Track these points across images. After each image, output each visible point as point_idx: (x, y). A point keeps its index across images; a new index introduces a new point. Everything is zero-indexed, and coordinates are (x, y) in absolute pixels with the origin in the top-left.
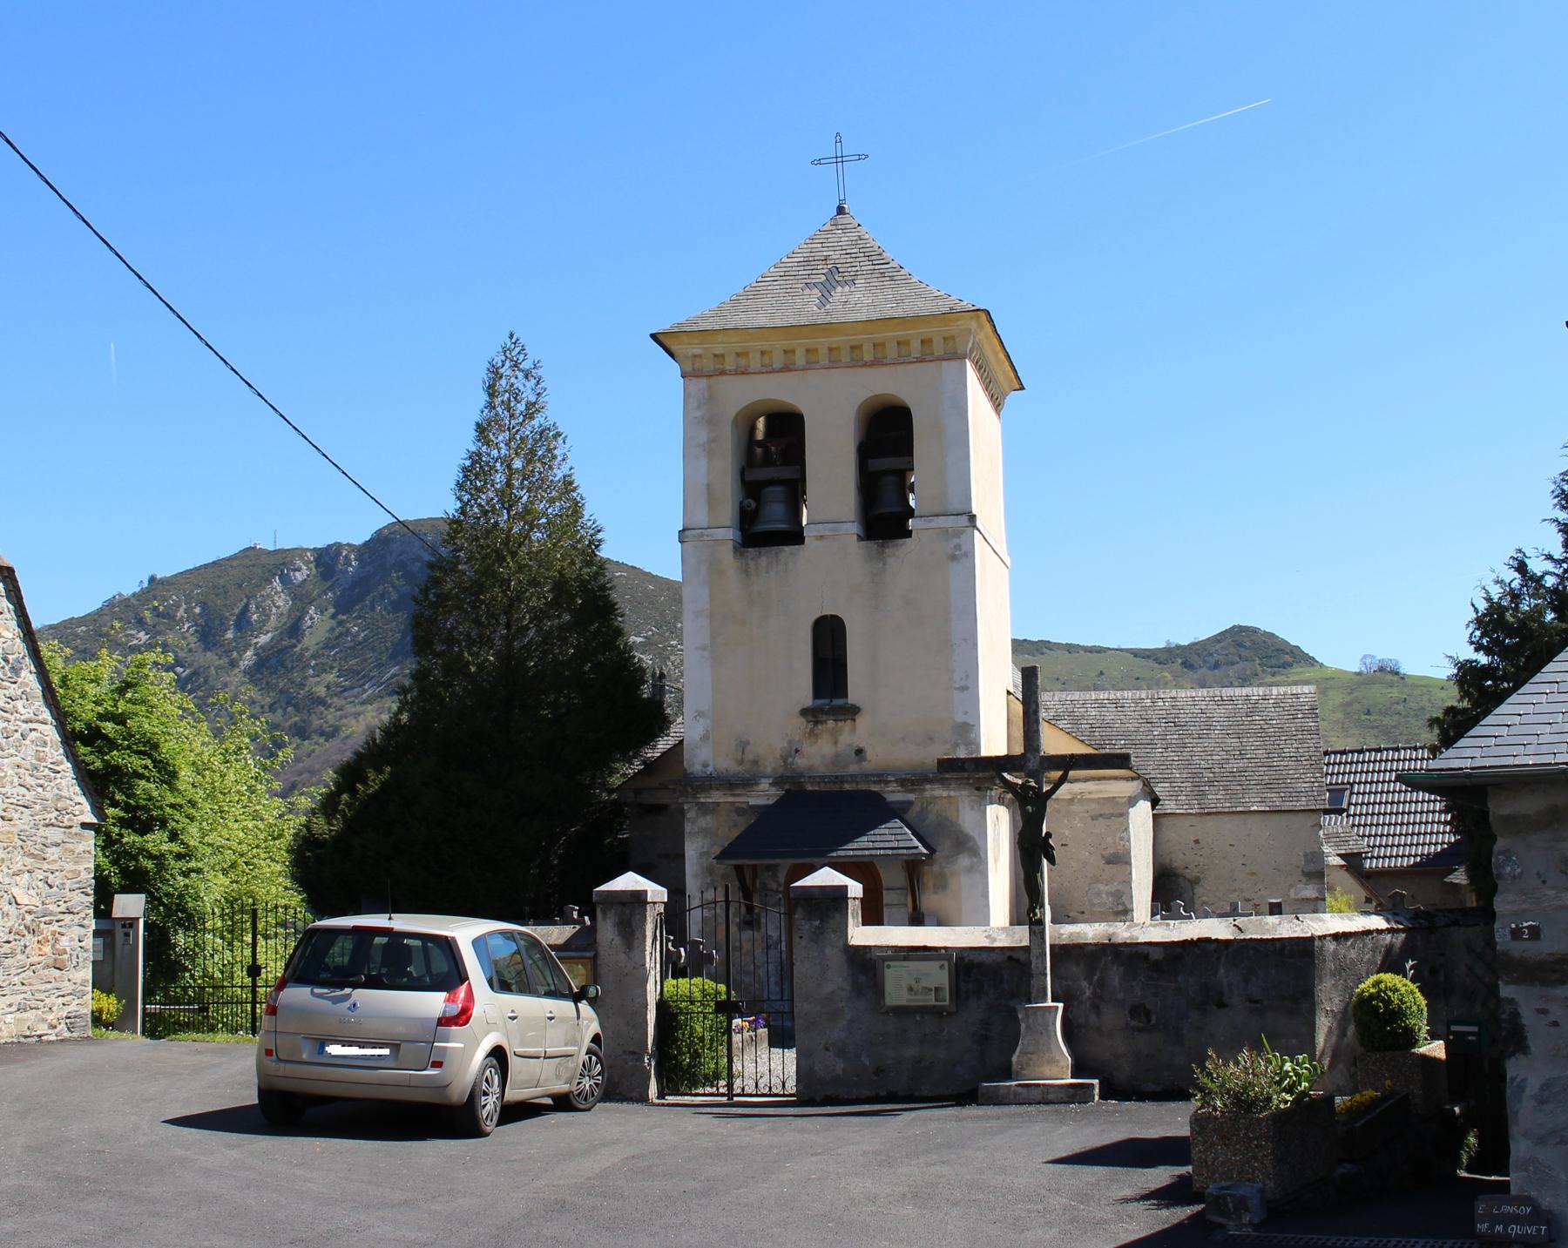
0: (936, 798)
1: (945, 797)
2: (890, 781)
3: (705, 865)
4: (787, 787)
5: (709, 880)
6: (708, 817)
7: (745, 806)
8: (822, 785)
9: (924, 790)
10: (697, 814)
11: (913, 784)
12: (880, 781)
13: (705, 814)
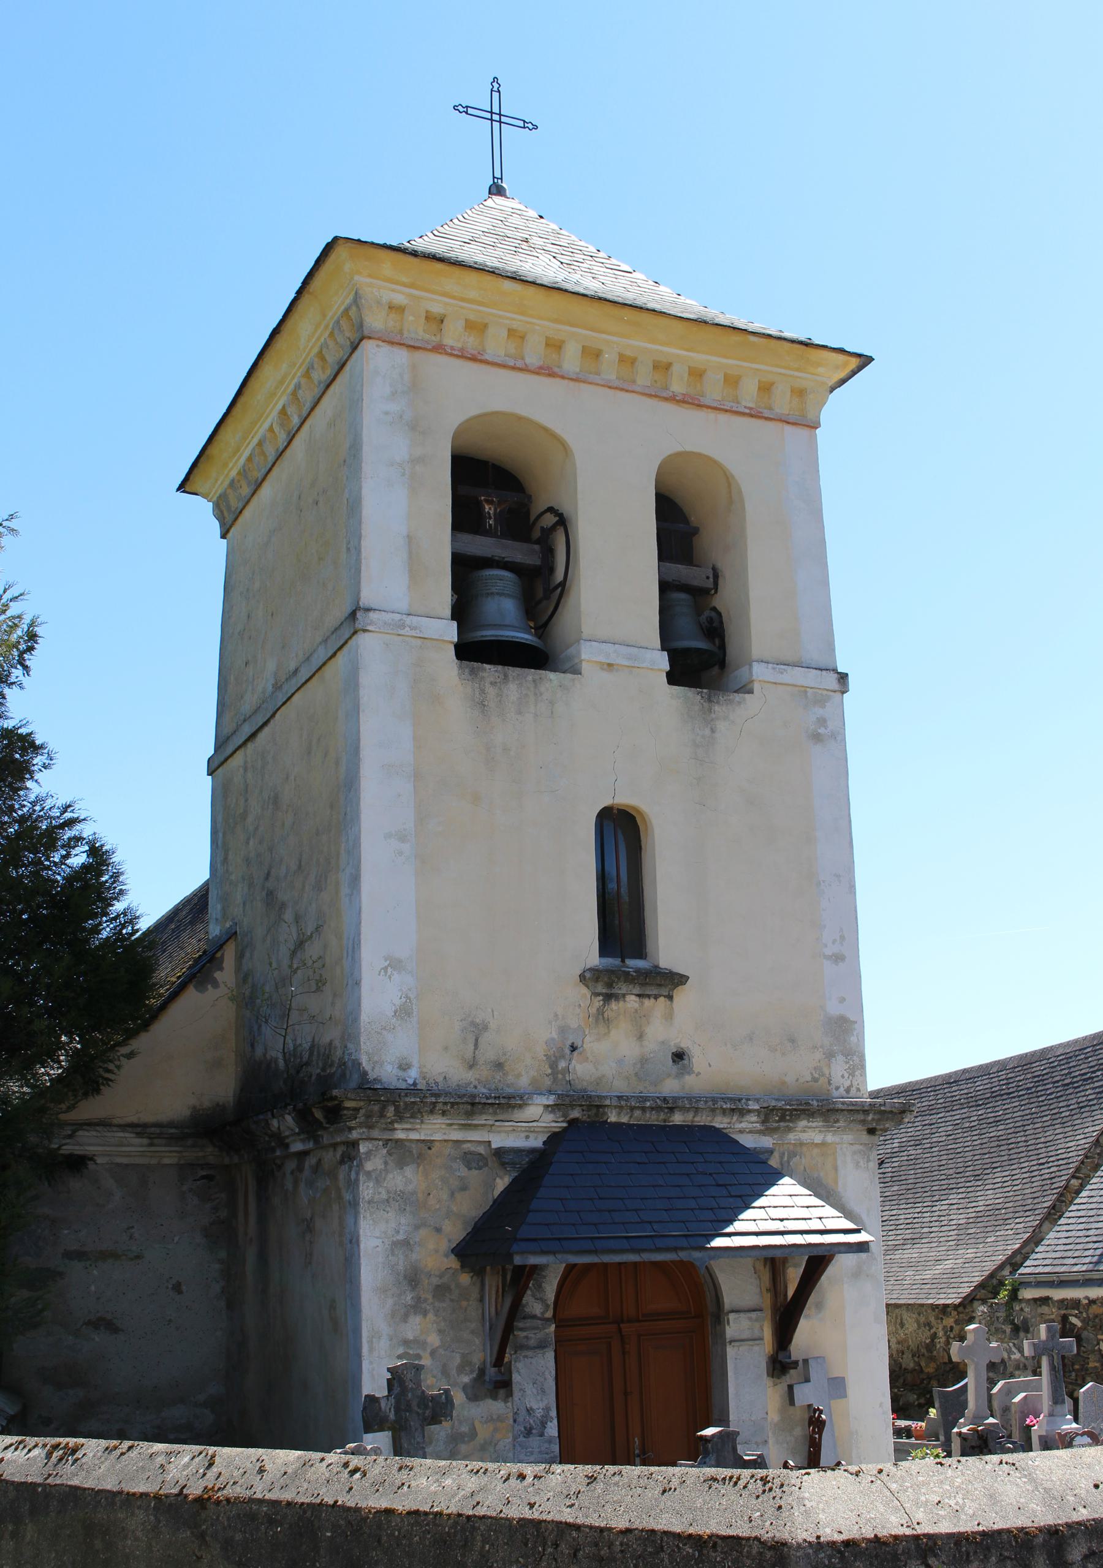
0: (802, 1144)
1: (817, 1145)
2: (749, 1111)
3: (401, 1268)
4: (575, 1114)
5: (409, 1298)
6: (409, 1171)
7: (481, 1149)
8: (637, 1113)
9: (789, 1130)
10: (386, 1163)
11: (782, 1119)
12: (733, 1110)
13: (401, 1164)
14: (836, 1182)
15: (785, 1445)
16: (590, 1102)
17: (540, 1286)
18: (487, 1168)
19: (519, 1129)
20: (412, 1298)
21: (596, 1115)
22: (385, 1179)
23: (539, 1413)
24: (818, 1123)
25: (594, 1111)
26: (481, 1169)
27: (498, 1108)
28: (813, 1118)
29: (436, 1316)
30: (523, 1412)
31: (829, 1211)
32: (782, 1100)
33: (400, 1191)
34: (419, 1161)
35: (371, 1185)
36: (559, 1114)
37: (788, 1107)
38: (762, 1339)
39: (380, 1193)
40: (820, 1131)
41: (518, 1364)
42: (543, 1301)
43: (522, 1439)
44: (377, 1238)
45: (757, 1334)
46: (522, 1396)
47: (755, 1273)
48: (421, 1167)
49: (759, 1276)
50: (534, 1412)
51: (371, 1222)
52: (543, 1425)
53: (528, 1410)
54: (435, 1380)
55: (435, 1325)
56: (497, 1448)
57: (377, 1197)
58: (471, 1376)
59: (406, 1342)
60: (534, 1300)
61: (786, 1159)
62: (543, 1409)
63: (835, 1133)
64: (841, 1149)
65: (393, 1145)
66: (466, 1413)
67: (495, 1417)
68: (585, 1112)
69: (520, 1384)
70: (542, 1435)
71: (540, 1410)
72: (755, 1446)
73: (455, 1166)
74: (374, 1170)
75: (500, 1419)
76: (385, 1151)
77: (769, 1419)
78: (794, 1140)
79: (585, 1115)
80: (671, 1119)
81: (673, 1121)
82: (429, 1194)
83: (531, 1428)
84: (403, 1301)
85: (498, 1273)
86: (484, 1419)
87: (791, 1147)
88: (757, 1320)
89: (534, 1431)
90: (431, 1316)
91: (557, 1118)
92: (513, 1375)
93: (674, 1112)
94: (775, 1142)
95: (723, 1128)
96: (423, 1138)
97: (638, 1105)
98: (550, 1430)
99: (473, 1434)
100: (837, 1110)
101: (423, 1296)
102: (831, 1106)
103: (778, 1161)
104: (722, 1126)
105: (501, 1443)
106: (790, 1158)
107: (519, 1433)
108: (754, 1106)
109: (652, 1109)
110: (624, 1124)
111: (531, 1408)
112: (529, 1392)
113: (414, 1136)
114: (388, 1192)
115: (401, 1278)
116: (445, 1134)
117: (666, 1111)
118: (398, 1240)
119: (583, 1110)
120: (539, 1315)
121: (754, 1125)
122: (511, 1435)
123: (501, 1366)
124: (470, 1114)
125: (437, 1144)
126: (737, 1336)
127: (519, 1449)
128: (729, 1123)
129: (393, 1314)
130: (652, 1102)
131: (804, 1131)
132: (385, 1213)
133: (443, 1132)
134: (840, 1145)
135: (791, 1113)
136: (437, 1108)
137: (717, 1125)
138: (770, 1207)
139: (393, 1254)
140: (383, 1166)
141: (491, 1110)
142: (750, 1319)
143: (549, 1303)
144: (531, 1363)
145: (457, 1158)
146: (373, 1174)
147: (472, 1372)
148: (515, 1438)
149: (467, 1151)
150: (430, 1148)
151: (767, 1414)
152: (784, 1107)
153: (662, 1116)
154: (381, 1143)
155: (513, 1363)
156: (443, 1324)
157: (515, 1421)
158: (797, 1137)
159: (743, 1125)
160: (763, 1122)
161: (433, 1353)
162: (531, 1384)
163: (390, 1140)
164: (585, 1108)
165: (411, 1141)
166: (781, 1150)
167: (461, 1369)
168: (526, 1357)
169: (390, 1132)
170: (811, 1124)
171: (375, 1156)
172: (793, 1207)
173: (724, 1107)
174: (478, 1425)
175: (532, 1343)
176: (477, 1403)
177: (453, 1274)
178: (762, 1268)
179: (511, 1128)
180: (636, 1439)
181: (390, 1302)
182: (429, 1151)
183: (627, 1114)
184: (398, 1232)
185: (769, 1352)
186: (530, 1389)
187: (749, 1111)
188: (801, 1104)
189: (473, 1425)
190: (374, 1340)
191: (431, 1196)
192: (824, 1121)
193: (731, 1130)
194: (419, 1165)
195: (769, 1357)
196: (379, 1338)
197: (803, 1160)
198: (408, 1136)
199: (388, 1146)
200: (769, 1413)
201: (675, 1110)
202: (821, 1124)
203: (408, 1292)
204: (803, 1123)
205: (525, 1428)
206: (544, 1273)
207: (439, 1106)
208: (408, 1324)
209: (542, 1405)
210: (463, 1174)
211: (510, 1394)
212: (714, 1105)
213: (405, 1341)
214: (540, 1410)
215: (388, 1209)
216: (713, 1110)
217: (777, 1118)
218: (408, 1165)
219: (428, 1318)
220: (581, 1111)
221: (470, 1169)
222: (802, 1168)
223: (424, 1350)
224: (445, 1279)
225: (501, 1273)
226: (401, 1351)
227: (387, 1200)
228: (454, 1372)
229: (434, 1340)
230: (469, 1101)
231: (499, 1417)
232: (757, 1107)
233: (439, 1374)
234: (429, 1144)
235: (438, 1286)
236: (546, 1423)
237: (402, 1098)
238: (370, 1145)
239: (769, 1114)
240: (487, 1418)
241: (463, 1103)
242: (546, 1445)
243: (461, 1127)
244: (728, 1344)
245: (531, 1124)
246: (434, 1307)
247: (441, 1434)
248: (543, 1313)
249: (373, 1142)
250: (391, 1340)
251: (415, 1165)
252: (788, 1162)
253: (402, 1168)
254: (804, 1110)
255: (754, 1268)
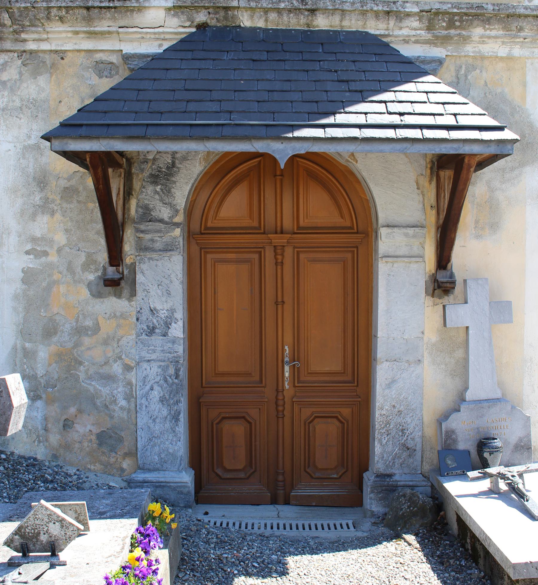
0: (483, 58)
1: (502, 58)
2: (408, 15)
3: (31, 170)
4: (201, 17)
5: (37, 198)
6: (42, 80)
7: (114, 59)
8: (273, 16)
9: (466, 39)
10: (21, 74)
11: (451, 25)
12: (388, 13)
13: (35, 74)
14: (524, 98)
15: (443, 366)
16: (214, 3)
17: (169, 191)
18: (118, 76)
19: (148, 36)
20: (41, 198)
21: (226, 18)
22: (19, 88)
23: (163, 314)
24: (496, 31)
25: (222, 13)
26: (111, 77)
27: (115, 12)
28: (489, 24)
29: (64, 216)
30: (146, 312)
31: (472, 108)
32: (448, 3)
33: (33, 99)
34: (51, 71)
35: (6, 93)
36: (183, 18)
37: (455, 10)
38: (422, 257)
39: (13, 101)
40: (503, 43)
41: (142, 266)
42: (171, 206)
43: (144, 337)
44: (10, 142)
45: (416, 250)
46: (146, 296)
47: (418, 189)
48: (54, 76)
49: (422, 192)
50: (157, 313)
51: (5, 127)
52: (168, 325)
53: (151, 310)
54: (60, 276)
55: (62, 225)
56: (120, 344)
57: (11, 104)
58: (96, 274)
59: (34, 240)
60: (161, 205)
61: (463, 72)
62: (167, 310)
63: (522, 45)
64: (532, 64)
65: (28, 56)
66: (90, 309)
67: (118, 314)
68: (211, 16)
69: (144, 285)
70: (165, 335)
71: (165, 311)
72: (406, 365)
73: (87, 74)
74: (9, 80)
75: (123, 316)
76: (20, 62)
77: (426, 339)
78: (473, 52)
79: (213, 19)
80: (315, 23)
81: (317, 26)
82: (60, 102)
83: (154, 328)
84: (32, 201)
85: (120, 176)
86: (108, 315)
87: (470, 61)
88: (414, 236)
89: (157, 331)
90: (58, 216)
91: (182, 22)
92: (137, 276)
93: (315, 15)
94: (449, 54)
95: (380, 35)
96: (53, 48)
97: (270, 6)
98: (175, 331)
99: (97, 329)
100: (520, 16)
101: (51, 197)
102: (511, 11)
103: (454, 74)
104: (377, 32)
105: (124, 339)
106: (468, 72)
107: (142, 331)
108: (412, 8)
109: (290, 11)
110: (260, 28)
111: (155, 309)
112: (152, 293)
113: (45, 46)
114: (22, 100)
115: (31, 180)
116: (76, 44)
117: (306, 13)
118: (29, 145)
119: (209, 13)
120: (166, 219)
121: (418, 32)
122: (134, 332)
123: (119, 266)
124: (89, 20)
125: (70, 54)
126: (391, 252)
127: (141, 346)
128: (387, 29)
129: (22, 213)
130: (287, 3)
131: (483, 42)
132: (18, 119)
133: (74, 42)
134: (530, 61)
135: (461, 17)
136: (52, 14)
137: (372, 32)
138: (393, 102)
139: (24, 158)
140: (18, 77)
141: (108, 15)
142: (406, 235)
143: (178, 208)
144: (156, 266)
145: (89, 68)
146: (8, 83)
147: (97, 270)
148: (138, 335)
149: (98, 60)
150: (62, 59)
151: (423, 333)
152: (450, 11)
153: (303, 20)
154: (16, 55)
155: (137, 264)
156: (70, 224)
157: (137, 319)
158: (477, 50)
159: (405, 32)
160: (429, 28)
161: (59, 250)
162: (156, 286)
163: (25, 51)
164: (211, 10)
165: (44, 51)
166: (458, 62)
167: (86, 267)
168: (150, 259)
169: (22, 44)
170: (488, 32)
171: (11, 67)
172: (425, 102)
173: (375, 8)
174: (101, 321)
175: (158, 245)
176: (102, 300)
177: (81, 177)
178: (427, 184)
179: (139, 36)
180: (286, 348)
181: (20, 201)
182: (62, 61)
183: (261, 17)
184: (29, 137)
185: (430, 271)
186: (154, 291)
187: (408, 15)
188: (472, 8)
189: (97, 319)
190: (4, 236)
191: (63, 103)
192: (504, 28)
193: (393, 39)
194: (51, 74)
195: (430, 276)
196: (9, 234)
197: (484, 74)
198: (39, 47)
199: (23, 57)
200: (425, 333)
201: (317, 13)
202: (501, 32)
203: (36, 193)
204: (478, 31)
205: (148, 327)
206: (173, 179)
207: (54, 12)
208: (36, 223)
209: (167, 306)
210: (94, 83)
211: (133, 293)
212: (362, 6)
213: (33, 238)
214: (165, 311)
215: (22, 116)
216: (364, 13)
217: (444, 24)
218: (42, 75)
219: (55, 218)
220: (206, 13)
221: (101, 77)
222: (483, 82)
223: (52, 247)
224: (73, 182)
225: (123, 176)
226: (29, 247)
227: (20, 108)
228: (79, 269)
229: (61, 238)
230: (82, 5)
231: (122, 315)
232: (416, 10)
233: (65, 270)
234: (61, 54)
235: (66, 189)
236: (170, 324)
237: (13, 4)
238: (6, 57)
239: (433, 19)
240: (111, 315)
241: (77, 7)
242: (170, 345)
243: (87, 35)
244: (380, 259)
245: (156, 30)
246: (62, 208)
247: (66, 326)
248: (171, 218)
249: (9, 53)
250: (20, 236)
251: (48, 75)
252: (466, 76)
253: (36, 78)
254: (477, 15)
255: (417, 184)
